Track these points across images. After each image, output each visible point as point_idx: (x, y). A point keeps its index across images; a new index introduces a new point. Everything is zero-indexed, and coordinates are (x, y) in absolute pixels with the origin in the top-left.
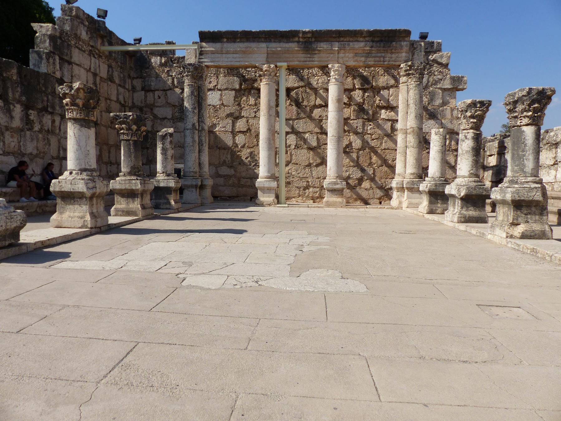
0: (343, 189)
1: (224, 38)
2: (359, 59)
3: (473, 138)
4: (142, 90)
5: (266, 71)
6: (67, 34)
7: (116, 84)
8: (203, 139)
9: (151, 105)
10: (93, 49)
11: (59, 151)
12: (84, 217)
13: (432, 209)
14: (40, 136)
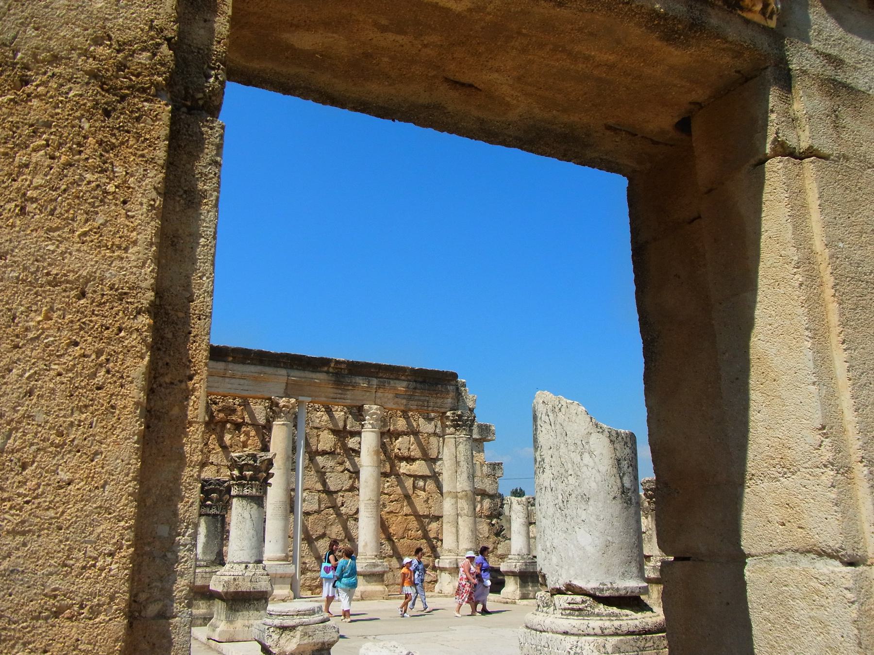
2: (399, 400)
5: (284, 406)
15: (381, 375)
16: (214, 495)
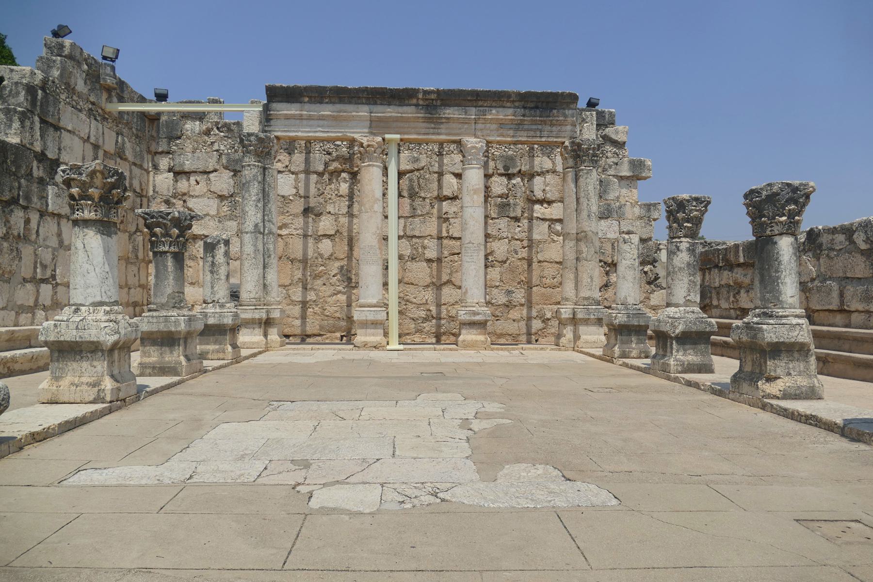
0: (486, 321)
3: (688, 250)
5: (369, 146)
6: (54, 82)
7: (129, 162)
8: (271, 247)
9: (185, 194)
10: (93, 107)
11: (35, 268)
12: (100, 384)
13: (624, 351)
14: (5, 245)
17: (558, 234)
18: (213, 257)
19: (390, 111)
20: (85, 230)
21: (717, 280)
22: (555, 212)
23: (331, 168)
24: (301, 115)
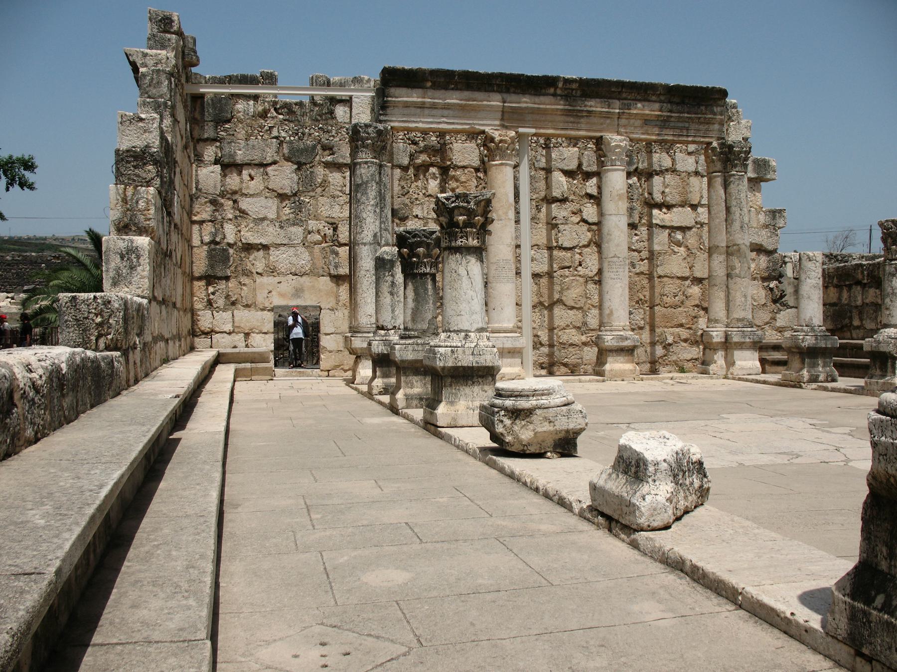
1: (427, 80)
4: (215, 163)
5: (501, 141)
9: (235, 192)
15: (624, 95)
16: (421, 250)
17: (679, 244)
18: (392, 275)
19: (526, 102)
20: (468, 257)
21: (859, 298)
22: (675, 219)
23: (419, 161)
24: (424, 103)
